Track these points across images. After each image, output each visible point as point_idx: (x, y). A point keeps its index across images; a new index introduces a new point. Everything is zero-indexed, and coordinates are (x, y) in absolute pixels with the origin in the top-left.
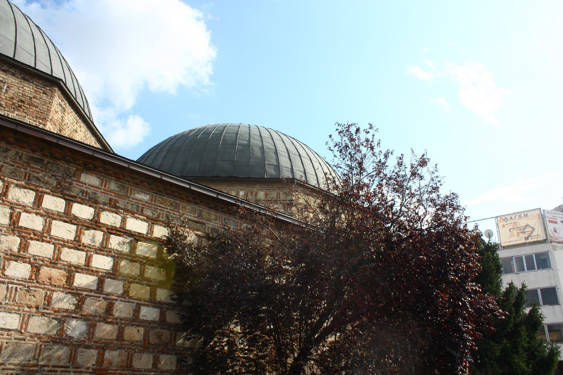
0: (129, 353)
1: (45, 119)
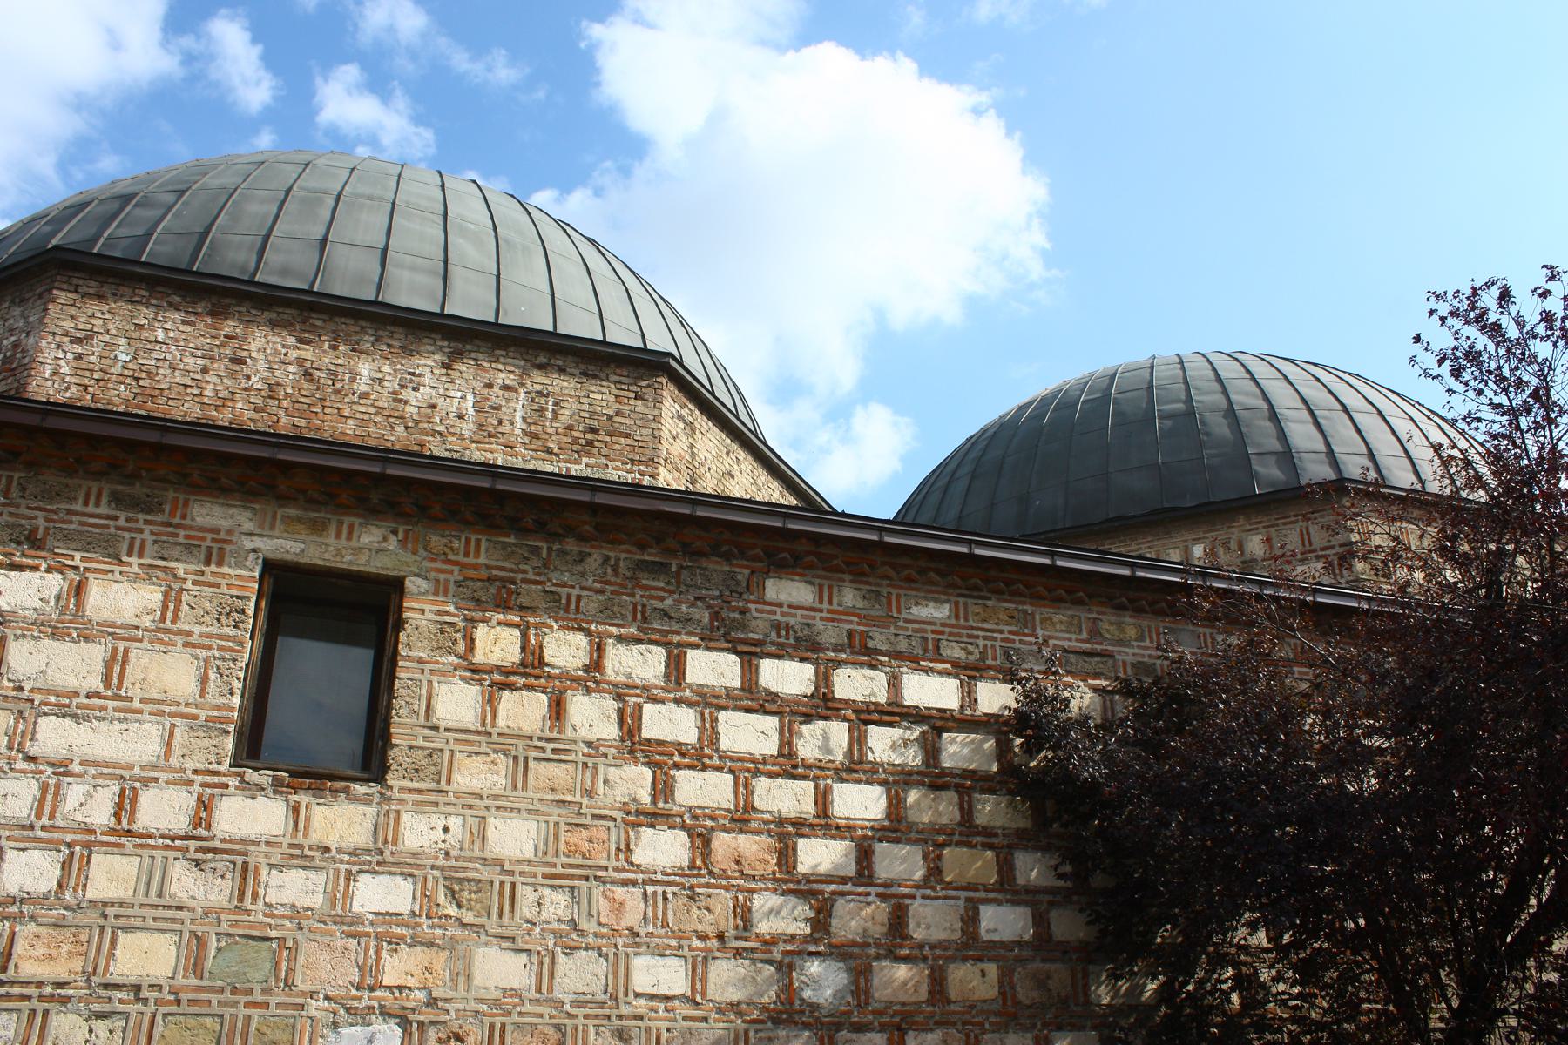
0: (968, 1036)
1: (651, 461)
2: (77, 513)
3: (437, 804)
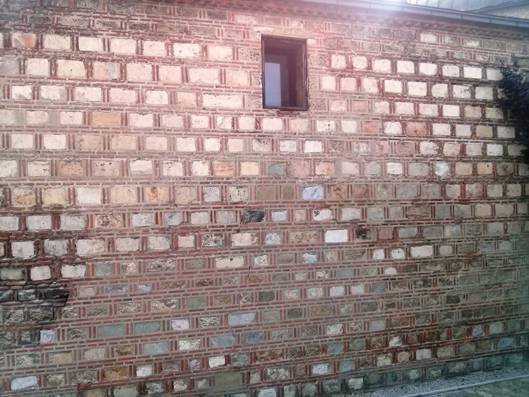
2: (199, 21)
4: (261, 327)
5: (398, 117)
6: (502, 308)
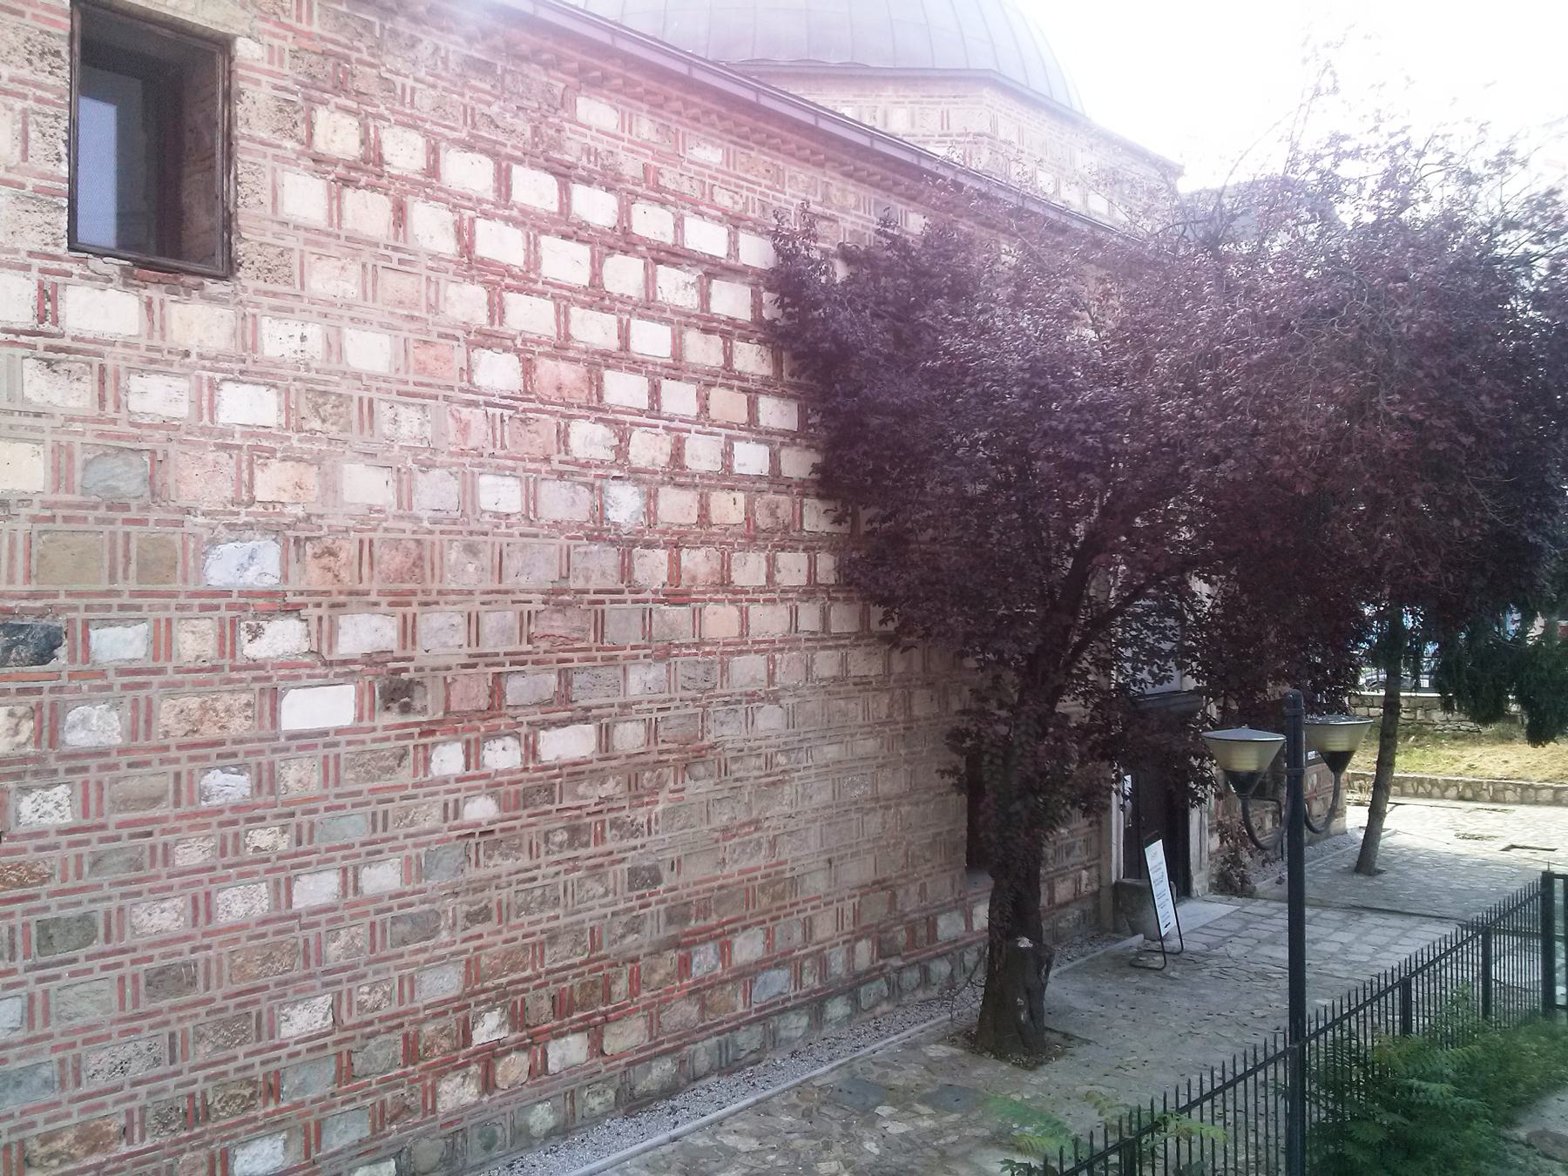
3: (292, 311)
4: (46, 1044)
5: (513, 339)
6: (763, 888)
